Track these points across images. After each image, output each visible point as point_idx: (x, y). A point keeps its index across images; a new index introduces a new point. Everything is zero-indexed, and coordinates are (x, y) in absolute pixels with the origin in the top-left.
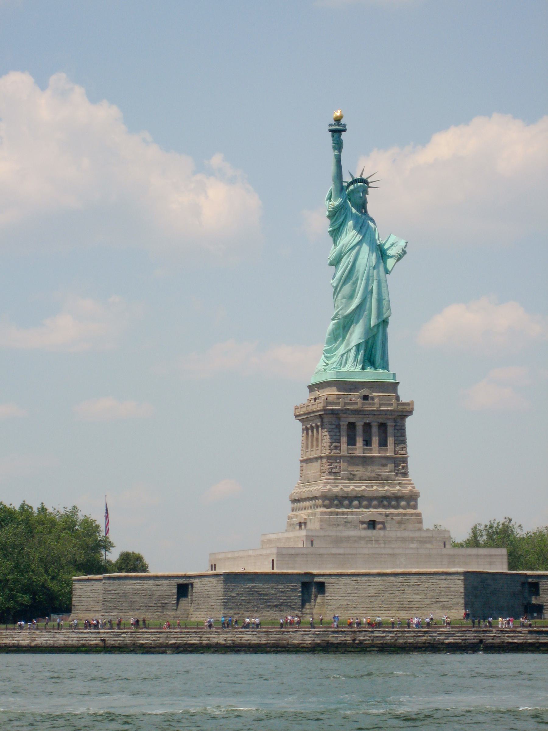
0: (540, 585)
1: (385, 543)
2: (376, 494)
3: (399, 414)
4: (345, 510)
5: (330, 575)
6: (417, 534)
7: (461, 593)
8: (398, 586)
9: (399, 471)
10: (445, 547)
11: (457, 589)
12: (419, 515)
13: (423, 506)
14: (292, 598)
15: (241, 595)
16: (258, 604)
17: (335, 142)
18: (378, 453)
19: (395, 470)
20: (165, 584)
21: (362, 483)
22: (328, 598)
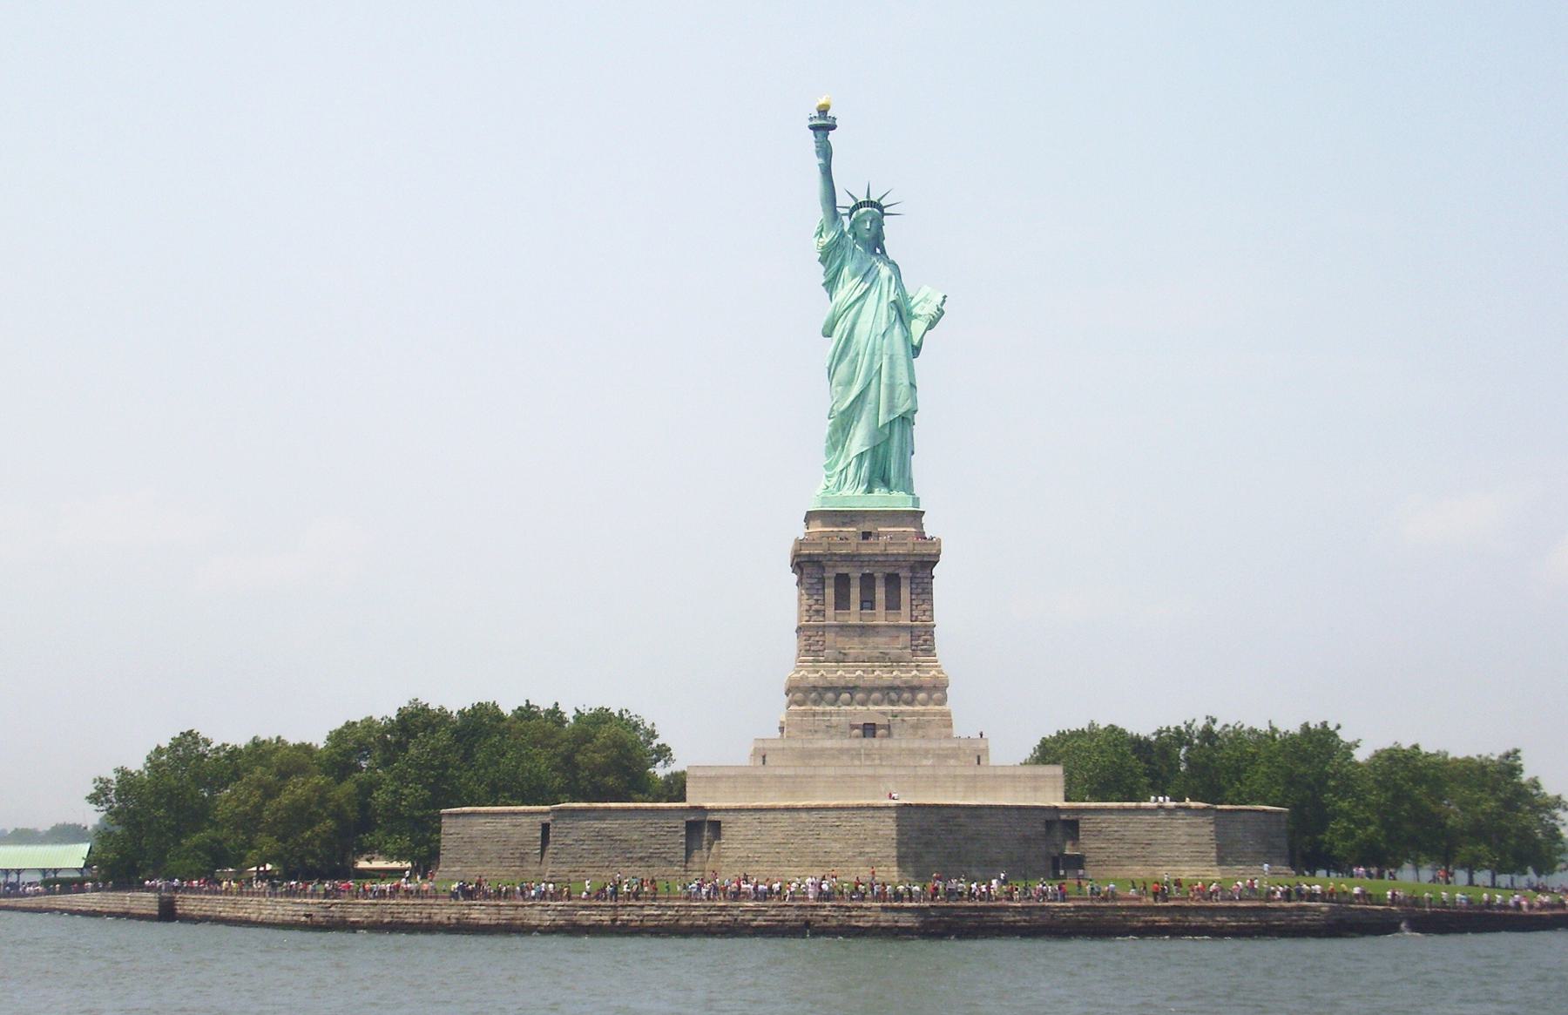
0: (1081, 825)
1: (880, 759)
2: (878, 683)
3: (918, 559)
4: (828, 708)
5: (727, 810)
6: (946, 744)
7: (893, 839)
8: (812, 828)
9: (919, 648)
10: (979, 763)
11: (887, 832)
12: (948, 714)
13: (955, 702)
14: (668, 846)
15: (581, 843)
16: (609, 857)
17: (819, 144)
18: (884, 619)
19: (912, 645)
20: (526, 825)
21: (857, 666)
22: (724, 846)
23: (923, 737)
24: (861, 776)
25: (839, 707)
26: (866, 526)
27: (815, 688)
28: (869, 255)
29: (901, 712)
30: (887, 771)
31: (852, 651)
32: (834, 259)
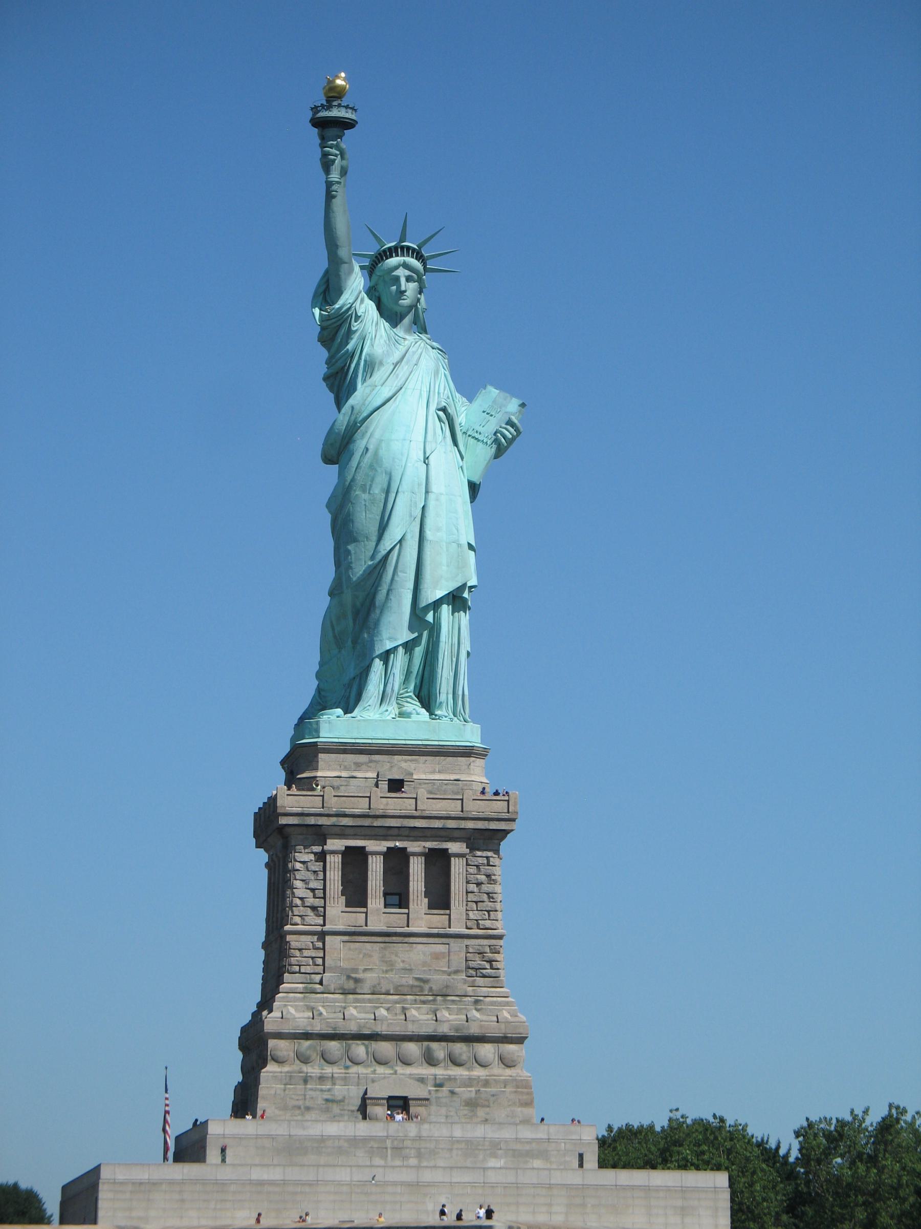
1: (419, 1155)
2: (411, 1029)
3: (480, 825)
4: (328, 1070)
10: (581, 1165)
19: (468, 968)
23: (486, 1120)
24: (395, 1184)
25: (347, 1068)
26: (395, 769)
27: (307, 1036)
28: (402, 334)
29: (450, 1079)
30: (438, 1176)
31: (368, 975)
32: (349, 333)
